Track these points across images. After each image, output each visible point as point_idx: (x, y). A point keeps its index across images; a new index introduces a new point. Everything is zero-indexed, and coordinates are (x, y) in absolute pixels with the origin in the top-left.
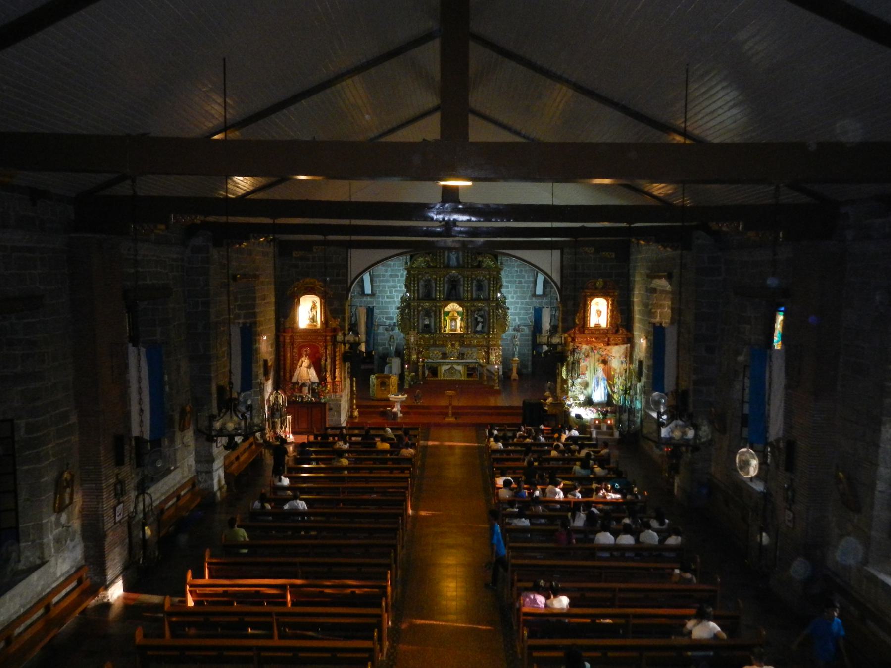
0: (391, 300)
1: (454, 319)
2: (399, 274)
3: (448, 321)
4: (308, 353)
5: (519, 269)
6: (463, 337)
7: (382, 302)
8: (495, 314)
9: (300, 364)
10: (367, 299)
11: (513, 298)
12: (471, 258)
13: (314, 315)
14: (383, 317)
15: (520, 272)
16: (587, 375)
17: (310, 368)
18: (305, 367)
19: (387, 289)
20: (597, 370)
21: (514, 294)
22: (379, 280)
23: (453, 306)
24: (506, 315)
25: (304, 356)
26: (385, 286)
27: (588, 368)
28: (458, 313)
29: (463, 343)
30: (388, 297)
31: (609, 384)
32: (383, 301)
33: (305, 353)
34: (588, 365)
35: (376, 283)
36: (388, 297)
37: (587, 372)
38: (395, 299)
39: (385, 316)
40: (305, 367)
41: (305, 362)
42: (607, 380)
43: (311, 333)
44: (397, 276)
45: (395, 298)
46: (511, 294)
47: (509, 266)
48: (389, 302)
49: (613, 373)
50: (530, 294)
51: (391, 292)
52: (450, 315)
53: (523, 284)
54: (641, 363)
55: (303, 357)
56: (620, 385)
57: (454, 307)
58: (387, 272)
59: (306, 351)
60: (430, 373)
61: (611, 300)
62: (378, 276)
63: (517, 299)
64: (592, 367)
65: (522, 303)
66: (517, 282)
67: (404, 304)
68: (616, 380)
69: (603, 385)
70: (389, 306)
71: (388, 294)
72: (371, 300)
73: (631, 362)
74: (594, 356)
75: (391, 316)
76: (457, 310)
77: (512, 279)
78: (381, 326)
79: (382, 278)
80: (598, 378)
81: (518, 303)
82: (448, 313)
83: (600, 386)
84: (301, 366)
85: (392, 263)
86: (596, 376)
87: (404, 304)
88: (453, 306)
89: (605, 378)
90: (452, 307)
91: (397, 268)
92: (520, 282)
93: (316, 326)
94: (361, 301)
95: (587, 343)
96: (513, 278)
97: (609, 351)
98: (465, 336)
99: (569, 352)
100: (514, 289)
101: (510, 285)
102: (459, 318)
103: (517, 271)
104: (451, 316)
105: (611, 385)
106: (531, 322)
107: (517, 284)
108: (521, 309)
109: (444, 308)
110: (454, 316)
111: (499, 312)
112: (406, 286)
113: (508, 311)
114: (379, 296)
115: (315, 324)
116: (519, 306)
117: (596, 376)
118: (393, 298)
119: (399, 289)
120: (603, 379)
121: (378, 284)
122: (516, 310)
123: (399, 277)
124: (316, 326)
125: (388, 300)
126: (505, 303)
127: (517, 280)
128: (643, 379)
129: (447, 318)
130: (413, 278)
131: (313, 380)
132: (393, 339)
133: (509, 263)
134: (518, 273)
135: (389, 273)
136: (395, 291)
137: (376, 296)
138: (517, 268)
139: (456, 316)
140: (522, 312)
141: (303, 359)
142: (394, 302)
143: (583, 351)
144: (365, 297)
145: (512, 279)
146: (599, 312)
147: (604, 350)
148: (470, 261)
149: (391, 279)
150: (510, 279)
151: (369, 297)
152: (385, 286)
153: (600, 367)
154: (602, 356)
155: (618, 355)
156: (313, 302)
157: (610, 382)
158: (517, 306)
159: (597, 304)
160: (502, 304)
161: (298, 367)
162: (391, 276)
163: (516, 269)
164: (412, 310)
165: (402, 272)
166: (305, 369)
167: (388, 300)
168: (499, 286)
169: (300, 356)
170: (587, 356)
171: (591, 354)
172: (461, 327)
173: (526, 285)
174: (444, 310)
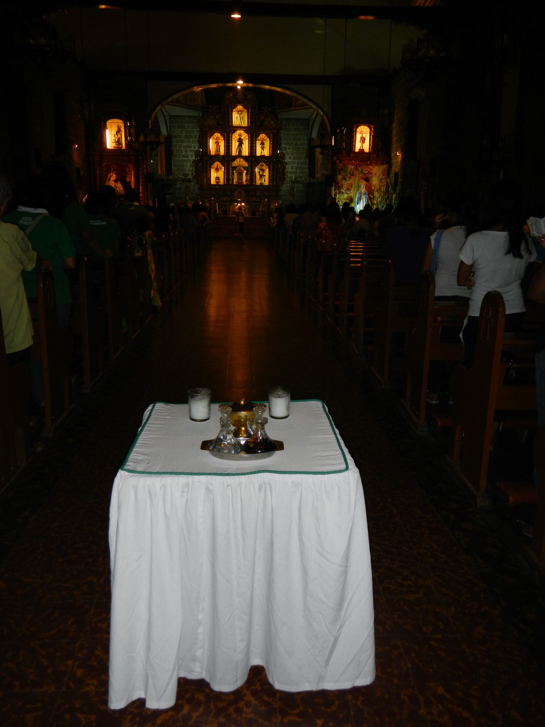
0: (186, 159)
1: (240, 174)
2: (193, 135)
3: (236, 174)
4: (115, 169)
7: (179, 160)
9: (108, 178)
11: (290, 158)
13: (119, 138)
14: (180, 174)
16: (351, 191)
17: (117, 182)
18: (113, 181)
19: (182, 149)
20: (360, 187)
21: (292, 155)
23: (240, 161)
24: (284, 168)
25: (112, 172)
26: (181, 145)
27: (353, 186)
28: (245, 168)
30: (184, 156)
31: (369, 197)
32: (180, 159)
33: (113, 169)
34: (353, 183)
36: (184, 156)
37: (352, 189)
38: (190, 158)
39: (181, 173)
40: (113, 181)
41: (113, 177)
42: (368, 195)
43: (117, 151)
44: (191, 137)
45: (190, 157)
46: (289, 154)
48: (185, 160)
49: (373, 188)
50: (305, 156)
51: (186, 151)
52: (237, 169)
53: (299, 146)
54: (396, 174)
55: (111, 172)
56: (379, 197)
57: (241, 162)
58: (182, 133)
59: (113, 167)
60: (220, 212)
61: (373, 128)
63: (293, 159)
64: (356, 185)
65: (298, 163)
66: (294, 144)
67: (197, 158)
68: (376, 194)
69: (364, 199)
70: (185, 164)
71: (184, 153)
73: (388, 176)
74: (358, 175)
75: (187, 172)
78: (179, 182)
79: (178, 139)
80: (360, 193)
81: (294, 163)
82: (235, 168)
83: (362, 200)
84: (109, 180)
85: (187, 125)
86: (359, 192)
87: (197, 158)
88: (240, 161)
89: (367, 193)
90: (239, 162)
91: (191, 129)
92: (296, 144)
93: (121, 148)
95: (352, 164)
97: (371, 169)
99: (338, 171)
101: (287, 146)
103: (294, 134)
104: (238, 170)
105: (370, 198)
106: (305, 179)
107: (294, 146)
108: (297, 168)
110: (240, 170)
111: (279, 166)
112: (199, 142)
113: (287, 166)
114: (176, 155)
115: (120, 146)
116: (296, 165)
117: (359, 192)
118: (188, 157)
119: (193, 149)
120: (365, 194)
121: (175, 143)
122: (293, 169)
123: (192, 138)
124: (121, 148)
125: (184, 159)
126: (283, 158)
127: (294, 142)
128: (398, 188)
129: (234, 171)
131: (119, 192)
132: (189, 188)
135: (184, 134)
136: (190, 151)
140: (298, 170)
141: (111, 174)
142: (190, 161)
143: (349, 169)
146: (363, 139)
147: (366, 170)
149: (186, 139)
152: (181, 145)
153: (363, 185)
154: (364, 174)
155: (378, 173)
156: (118, 127)
157: (371, 196)
158: (294, 165)
159: (361, 132)
161: (107, 180)
162: (186, 137)
163: (293, 132)
165: (196, 133)
166: (113, 182)
167: (184, 159)
168: (278, 144)
169: (109, 172)
170: (353, 174)
171: (356, 173)
172: (246, 181)
173: (301, 147)
174: (232, 164)
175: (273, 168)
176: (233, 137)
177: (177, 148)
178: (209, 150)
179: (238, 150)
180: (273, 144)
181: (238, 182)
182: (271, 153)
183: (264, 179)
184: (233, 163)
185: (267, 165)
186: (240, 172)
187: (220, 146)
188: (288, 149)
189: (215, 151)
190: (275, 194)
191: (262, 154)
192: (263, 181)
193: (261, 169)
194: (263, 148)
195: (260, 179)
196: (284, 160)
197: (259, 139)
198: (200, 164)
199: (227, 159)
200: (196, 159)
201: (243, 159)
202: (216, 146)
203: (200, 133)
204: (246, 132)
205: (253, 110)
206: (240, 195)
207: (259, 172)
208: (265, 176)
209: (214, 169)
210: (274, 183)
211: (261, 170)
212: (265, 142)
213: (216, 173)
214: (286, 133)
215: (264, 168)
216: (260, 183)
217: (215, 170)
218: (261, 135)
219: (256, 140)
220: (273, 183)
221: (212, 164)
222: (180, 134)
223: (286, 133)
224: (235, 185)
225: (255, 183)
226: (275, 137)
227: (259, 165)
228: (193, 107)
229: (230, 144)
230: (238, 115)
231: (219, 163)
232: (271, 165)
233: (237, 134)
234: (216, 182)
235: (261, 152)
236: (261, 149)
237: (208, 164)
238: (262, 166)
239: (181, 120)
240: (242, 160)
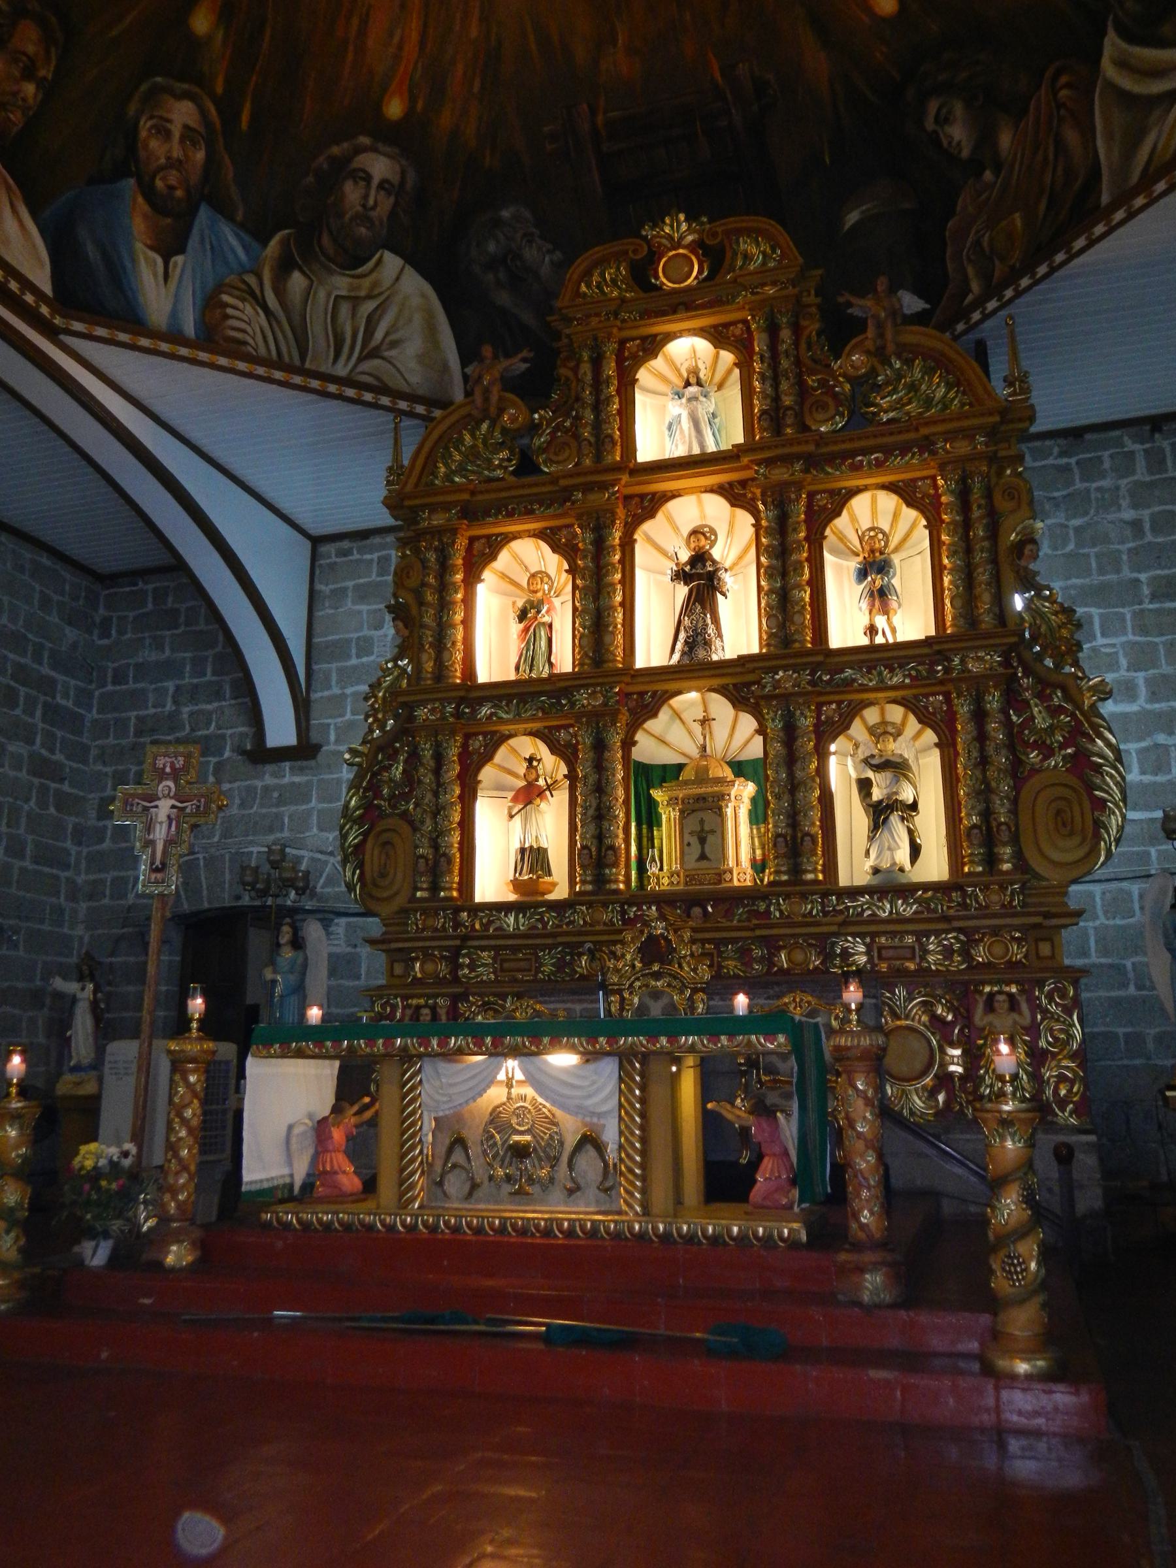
3: (668, 816)
5: (1146, 514)
6: (767, 913)
8: (993, 725)
10: (278, 775)
12: (801, 383)
15: (1155, 529)
21: (1134, 667)
22: (340, 671)
28: (740, 768)
29: (769, 961)
35: (329, 688)
47: (1077, 503)
57: (720, 732)
62: (339, 650)
63: (1154, 697)
66: (1146, 591)
67: (382, 727)
72: (297, 779)
76: (743, 757)
77: (1112, 577)
78: (343, 921)
79: (354, 661)
82: (669, 773)
87: (382, 727)
90: (697, 729)
94: (250, 790)
96: (1118, 571)
98: (779, 908)
100: (1131, 637)
101: (1094, 611)
102: (746, 790)
103: (1136, 525)
104: (686, 783)
109: (635, 724)
110: (702, 777)
112: (399, 612)
121: (336, 690)
127: (1143, 577)
129: (658, 795)
130: (432, 557)
133: (1079, 485)
134: (1149, 537)
137: (321, 757)
138: (1135, 506)
139: (720, 781)
144: (270, 768)
145: (1112, 577)
148: (787, 401)
150: (1096, 579)
151: (287, 765)
160: (1049, 662)
163: (1129, 515)
164: (428, 754)
172: (759, 867)
174: (628, 744)
175: (982, 737)
176: (642, 553)
177: (348, 716)
178: (459, 656)
179: (682, 636)
180: (966, 549)
181: (690, 878)
182: (949, 618)
183: (911, 833)
184: (639, 736)
185: (925, 719)
186: (701, 798)
187: (550, 626)
188: (1103, 635)
189: (517, 668)
190: (1017, 953)
191: (879, 640)
192: (903, 855)
193: (874, 762)
194: (881, 598)
195: (871, 839)
196: (1076, 664)
197: (842, 538)
198: (398, 771)
199: (583, 698)
200: (371, 731)
201: (722, 691)
202: (526, 630)
203: (404, 556)
204: (734, 495)
205: (786, 334)
206: (657, 976)
207: (865, 786)
208: (914, 807)
209: (510, 795)
210: (1003, 861)
211: (877, 768)
212: (896, 559)
213: (517, 819)
214: (1076, 522)
215: (899, 748)
216: (876, 871)
217: (515, 799)
218: (860, 505)
219: (816, 542)
220: (991, 861)
221: (488, 757)
222: (366, 632)
223: (1076, 522)
224: (664, 900)
225: (831, 866)
226: (976, 495)
227: (857, 729)
228: (350, 392)
229: (610, 595)
230: (677, 409)
231: (543, 751)
232: (963, 709)
233: (676, 529)
234: (517, 885)
235: (872, 630)
236: (864, 605)
237: (453, 752)
238: (880, 732)
239: (375, 556)
240: (721, 707)
